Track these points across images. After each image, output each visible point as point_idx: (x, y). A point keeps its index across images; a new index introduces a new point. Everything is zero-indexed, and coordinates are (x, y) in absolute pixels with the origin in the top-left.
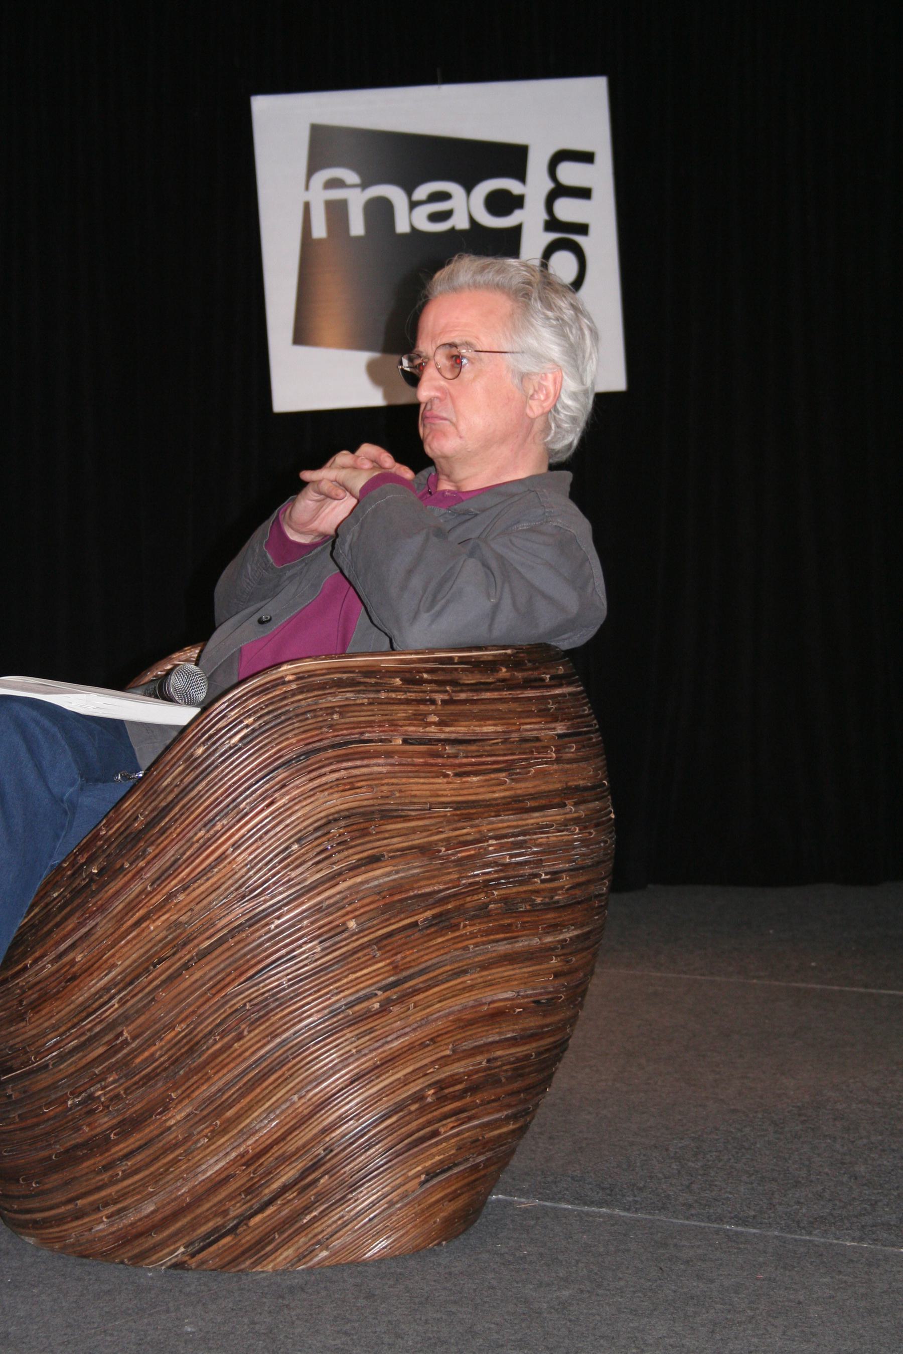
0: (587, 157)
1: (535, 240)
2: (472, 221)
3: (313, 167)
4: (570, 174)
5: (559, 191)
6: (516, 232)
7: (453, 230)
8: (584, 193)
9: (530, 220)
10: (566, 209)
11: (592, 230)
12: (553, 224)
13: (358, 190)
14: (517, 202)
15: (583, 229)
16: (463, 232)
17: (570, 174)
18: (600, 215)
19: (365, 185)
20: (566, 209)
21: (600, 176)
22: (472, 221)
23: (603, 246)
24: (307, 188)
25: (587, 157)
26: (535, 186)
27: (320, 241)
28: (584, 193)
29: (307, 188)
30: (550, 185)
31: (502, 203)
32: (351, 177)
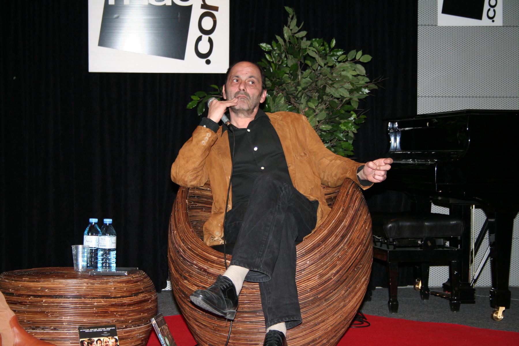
1: (196, 12)
6: (190, 8)
7: (165, 5)
15: (216, 9)
16: (169, 6)
27: (112, 6)
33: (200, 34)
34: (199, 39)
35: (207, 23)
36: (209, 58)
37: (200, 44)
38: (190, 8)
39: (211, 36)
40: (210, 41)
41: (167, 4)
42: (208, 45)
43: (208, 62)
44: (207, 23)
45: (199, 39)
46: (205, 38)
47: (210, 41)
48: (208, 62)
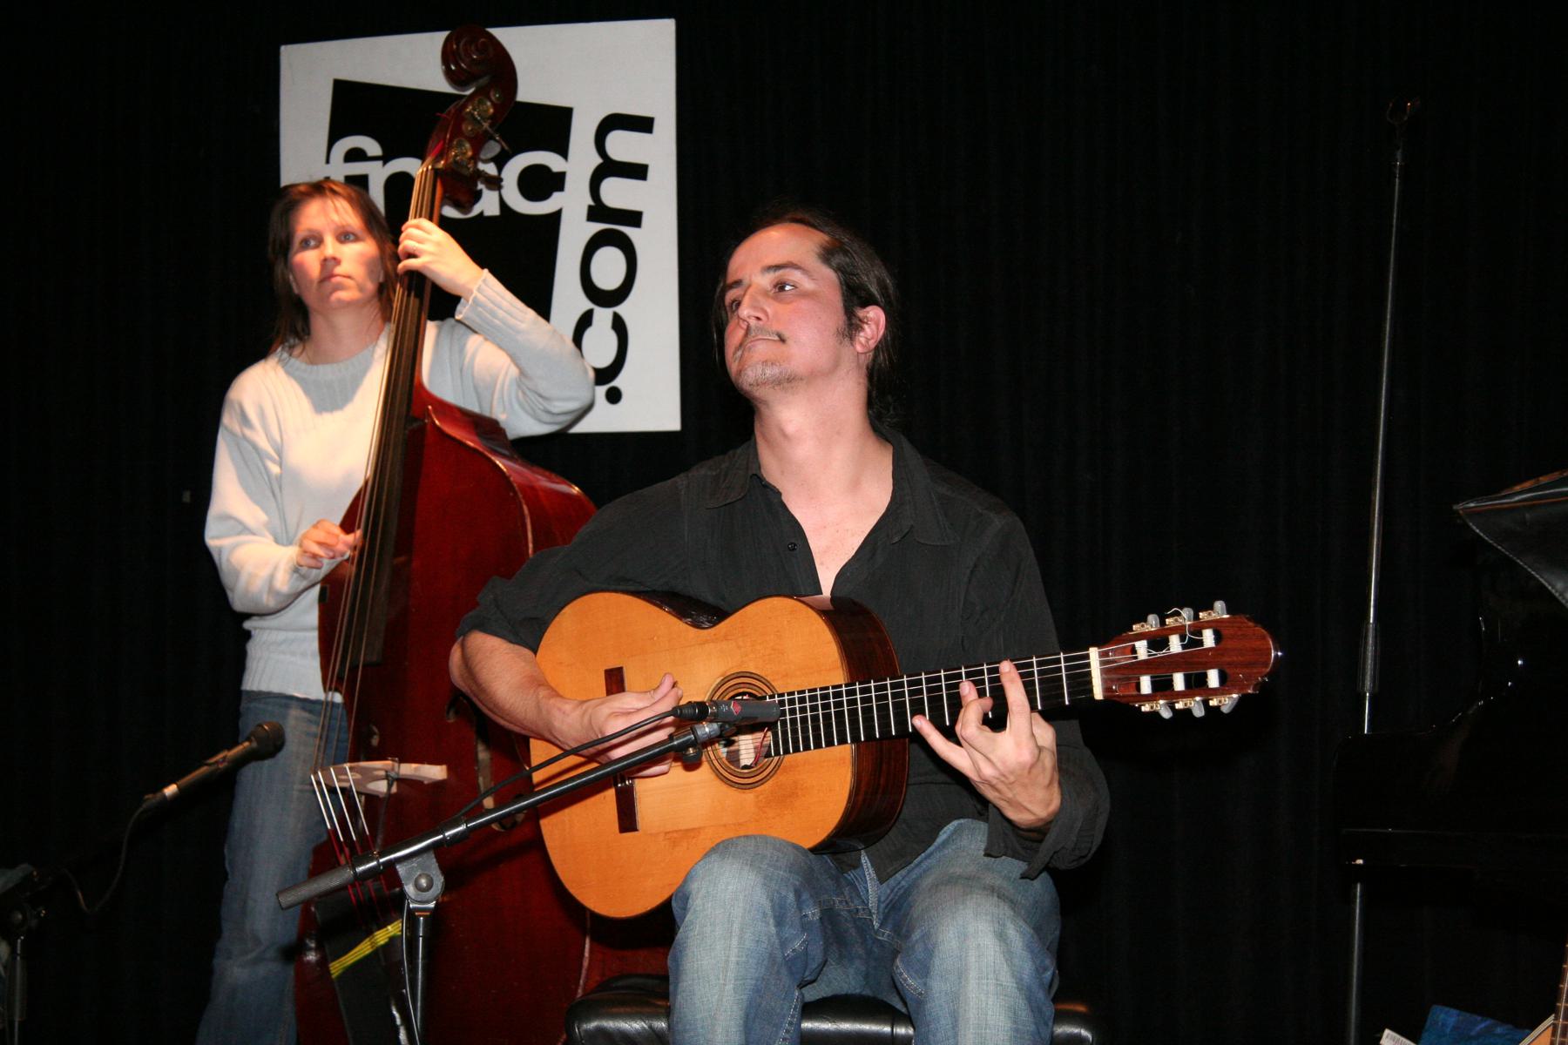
0: (644, 125)
1: (575, 233)
2: (503, 205)
3: (333, 138)
4: (622, 146)
5: (609, 168)
7: (482, 213)
8: (637, 172)
9: (571, 203)
10: (617, 193)
11: (645, 220)
12: (598, 211)
13: (380, 163)
14: (556, 182)
15: (634, 218)
17: (622, 146)
18: (656, 202)
19: (385, 158)
20: (617, 193)
21: (659, 149)
22: (503, 205)
23: (659, 243)
24: (328, 161)
25: (644, 125)
26: (579, 162)
28: (637, 172)
29: (328, 161)
30: (599, 161)
31: (540, 183)
32: (372, 147)
33: (586, 305)
34: (585, 321)
35: (609, 268)
36: (614, 383)
37: (589, 336)
38: (556, 217)
39: (621, 309)
40: (619, 326)
41: (487, 213)
42: (612, 340)
43: (614, 396)
44: (609, 268)
45: (585, 321)
46: (603, 316)
47: (619, 326)
48: (614, 396)
